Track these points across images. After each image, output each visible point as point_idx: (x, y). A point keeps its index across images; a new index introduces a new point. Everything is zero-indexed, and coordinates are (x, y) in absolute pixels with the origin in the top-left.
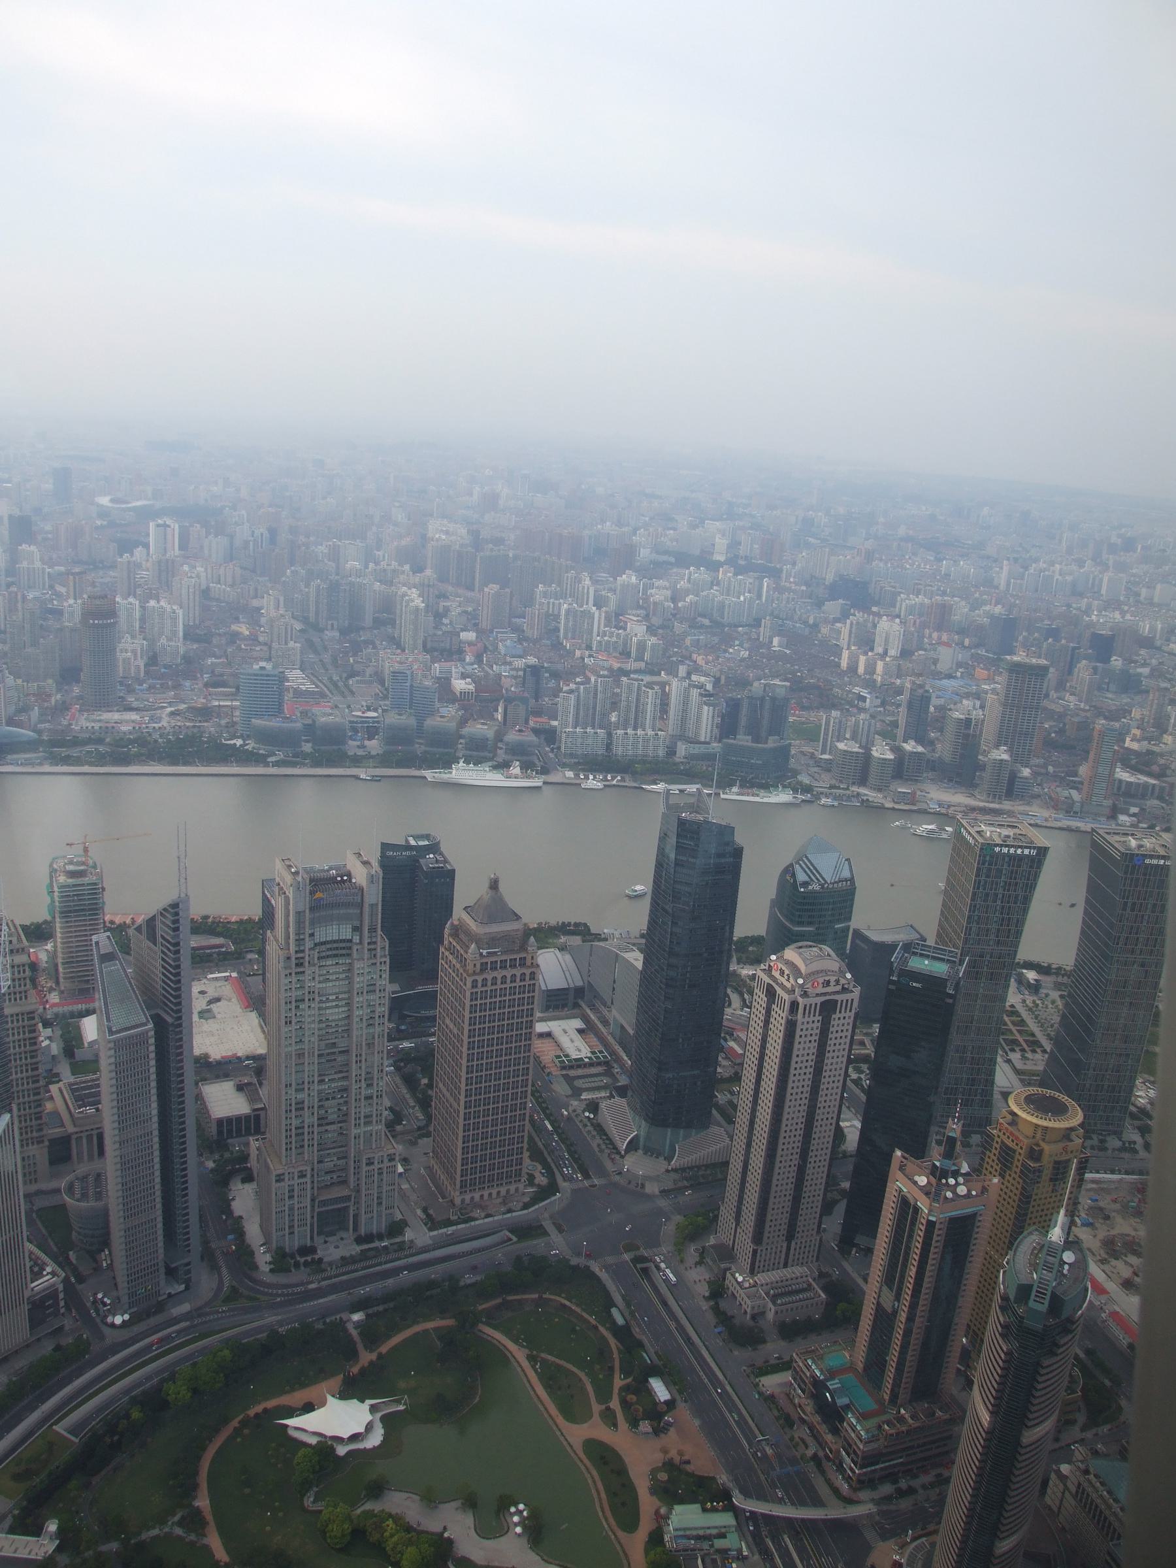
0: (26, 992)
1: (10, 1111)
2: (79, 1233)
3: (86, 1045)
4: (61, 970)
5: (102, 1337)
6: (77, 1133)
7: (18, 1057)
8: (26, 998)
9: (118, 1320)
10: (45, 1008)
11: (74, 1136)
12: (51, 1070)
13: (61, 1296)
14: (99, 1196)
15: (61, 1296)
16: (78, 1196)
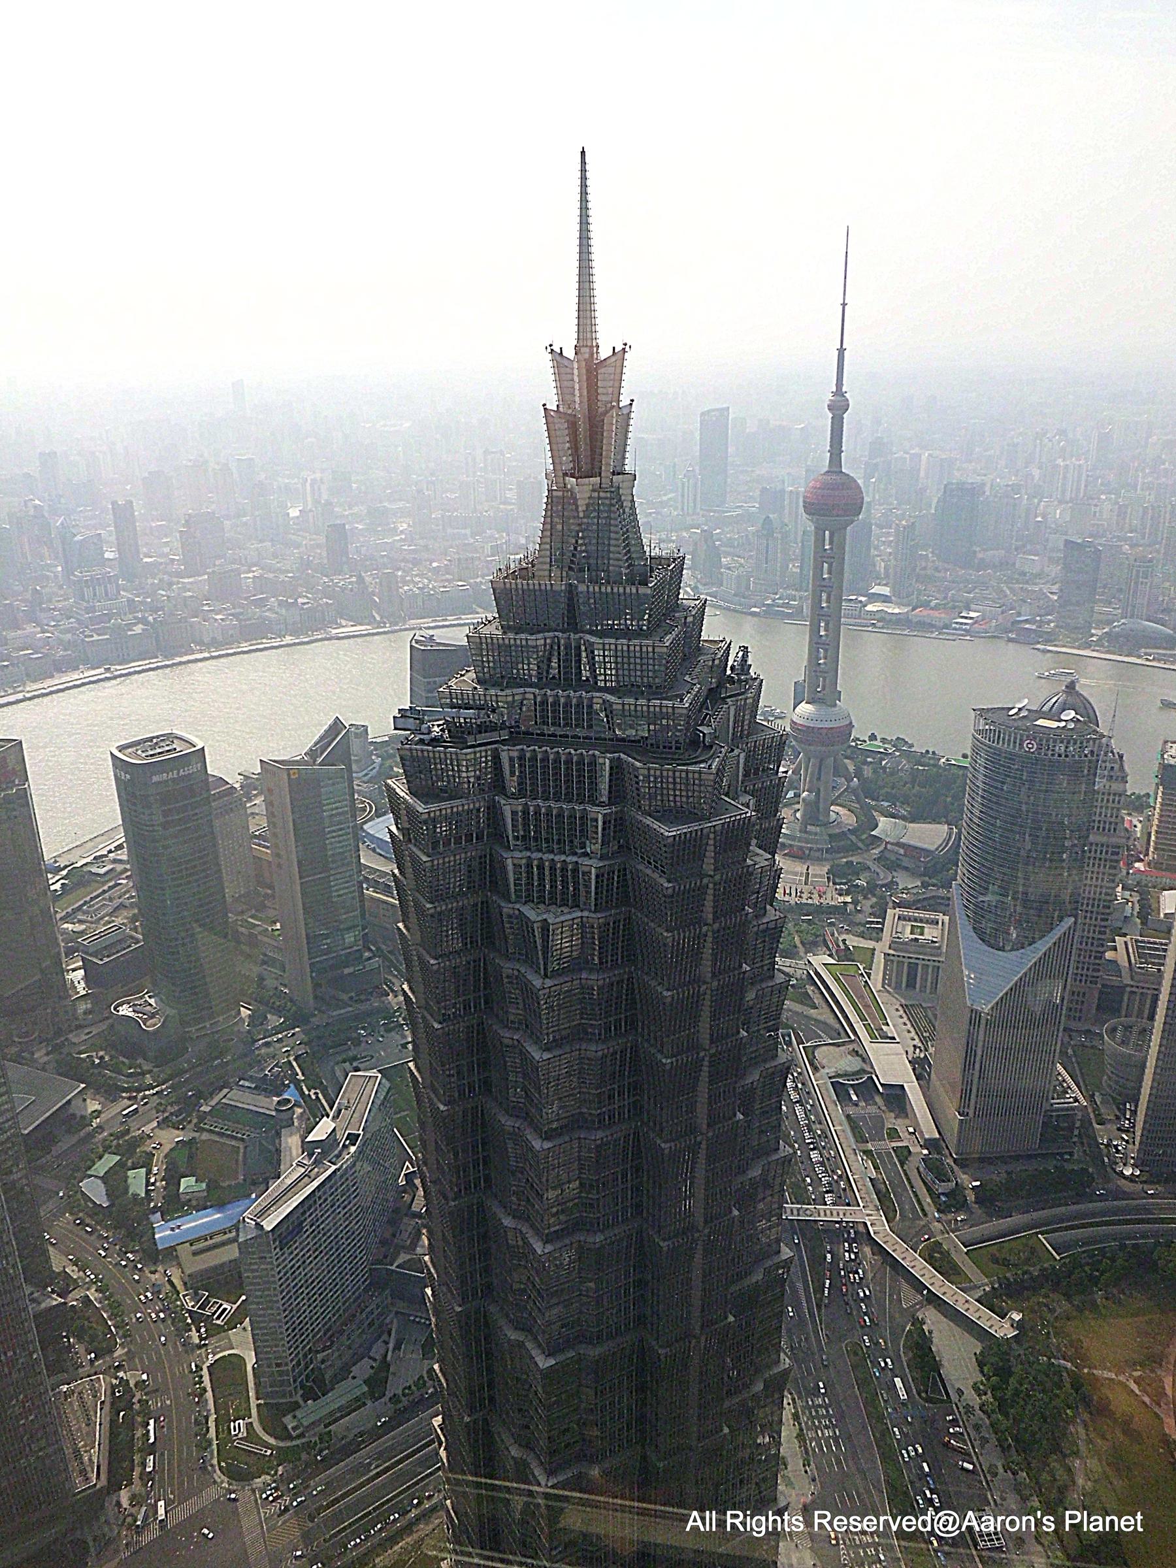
0: (1116, 824)
1: (1076, 917)
2: (1110, 1078)
3: (1162, 915)
4: (1153, 838)
5: (1107, 1180)
6: (1132, 986)
7: (1091, 902)
8: (1115, 829)
9: (1128, 1172)
10: (1128, 873)
11: (1128, 989)
12: (1121, 929)
13: (1078, 1124)
14: (1139, 1048)
15: (1078, 1124)
16: (1118, 1040)
